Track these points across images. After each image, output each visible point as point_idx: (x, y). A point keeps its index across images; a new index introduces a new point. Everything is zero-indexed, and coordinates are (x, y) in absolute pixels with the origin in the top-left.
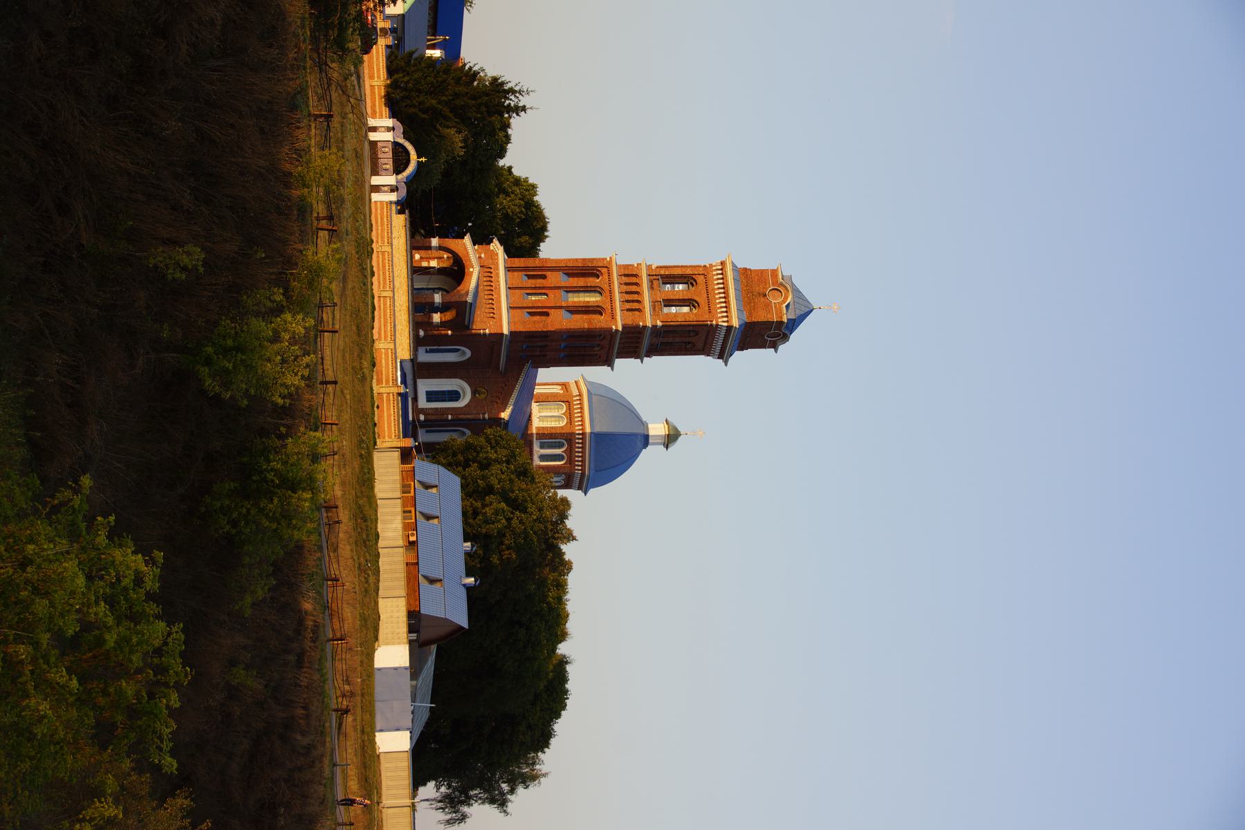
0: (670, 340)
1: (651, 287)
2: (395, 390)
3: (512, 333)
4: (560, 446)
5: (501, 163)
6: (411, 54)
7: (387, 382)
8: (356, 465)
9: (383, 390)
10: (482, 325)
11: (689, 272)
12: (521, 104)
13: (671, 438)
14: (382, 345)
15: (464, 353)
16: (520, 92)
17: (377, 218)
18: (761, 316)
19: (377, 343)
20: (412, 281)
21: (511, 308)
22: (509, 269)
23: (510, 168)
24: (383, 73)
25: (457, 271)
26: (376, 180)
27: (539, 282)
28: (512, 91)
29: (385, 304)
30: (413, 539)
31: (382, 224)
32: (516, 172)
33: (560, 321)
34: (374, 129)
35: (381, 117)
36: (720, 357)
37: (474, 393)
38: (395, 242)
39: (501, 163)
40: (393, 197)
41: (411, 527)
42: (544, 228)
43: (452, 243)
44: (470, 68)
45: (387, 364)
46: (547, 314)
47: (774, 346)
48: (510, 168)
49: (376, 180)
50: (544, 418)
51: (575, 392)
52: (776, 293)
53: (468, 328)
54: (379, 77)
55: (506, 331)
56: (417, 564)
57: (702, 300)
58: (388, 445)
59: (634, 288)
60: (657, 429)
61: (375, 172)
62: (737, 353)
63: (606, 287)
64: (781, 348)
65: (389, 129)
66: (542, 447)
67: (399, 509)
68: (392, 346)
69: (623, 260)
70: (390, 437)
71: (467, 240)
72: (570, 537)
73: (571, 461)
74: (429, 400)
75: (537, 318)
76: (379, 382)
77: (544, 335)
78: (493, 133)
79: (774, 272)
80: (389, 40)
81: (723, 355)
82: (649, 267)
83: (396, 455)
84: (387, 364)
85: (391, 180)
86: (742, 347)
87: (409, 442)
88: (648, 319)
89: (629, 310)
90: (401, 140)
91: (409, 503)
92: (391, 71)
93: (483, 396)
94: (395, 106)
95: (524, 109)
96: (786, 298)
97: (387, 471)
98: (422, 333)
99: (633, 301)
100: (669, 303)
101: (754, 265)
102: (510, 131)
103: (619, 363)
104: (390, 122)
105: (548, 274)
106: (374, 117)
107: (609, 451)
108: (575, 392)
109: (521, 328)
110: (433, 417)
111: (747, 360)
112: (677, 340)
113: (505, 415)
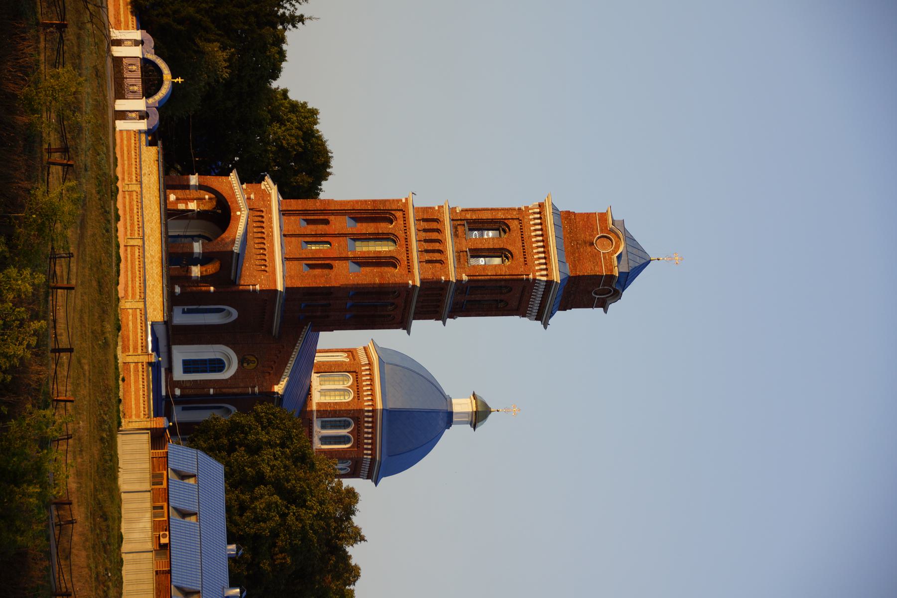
1: (455, 234)
2: (145, 359)
3: (287, 289)
10: (252, 280)
11: (500, 215)
26: (121, 105)
29: (133, 255)
30: (164, 541)
31: (129, 158)
34: (119, 43)
38: (145, 180)
40: (143, 125)
41: (161, 526)
46: (330, 267)
56: (170, 572)
61: (120, 95)
67: (148, 505)
68: (141, 305)
76: (125, 349)
82: (452, 210)
87: (161, 422)
91: (161, 497)
96: (617, 247)
97: (134, 456)
104: (137, 35)
106: (118, 28)
109: (298, 284)
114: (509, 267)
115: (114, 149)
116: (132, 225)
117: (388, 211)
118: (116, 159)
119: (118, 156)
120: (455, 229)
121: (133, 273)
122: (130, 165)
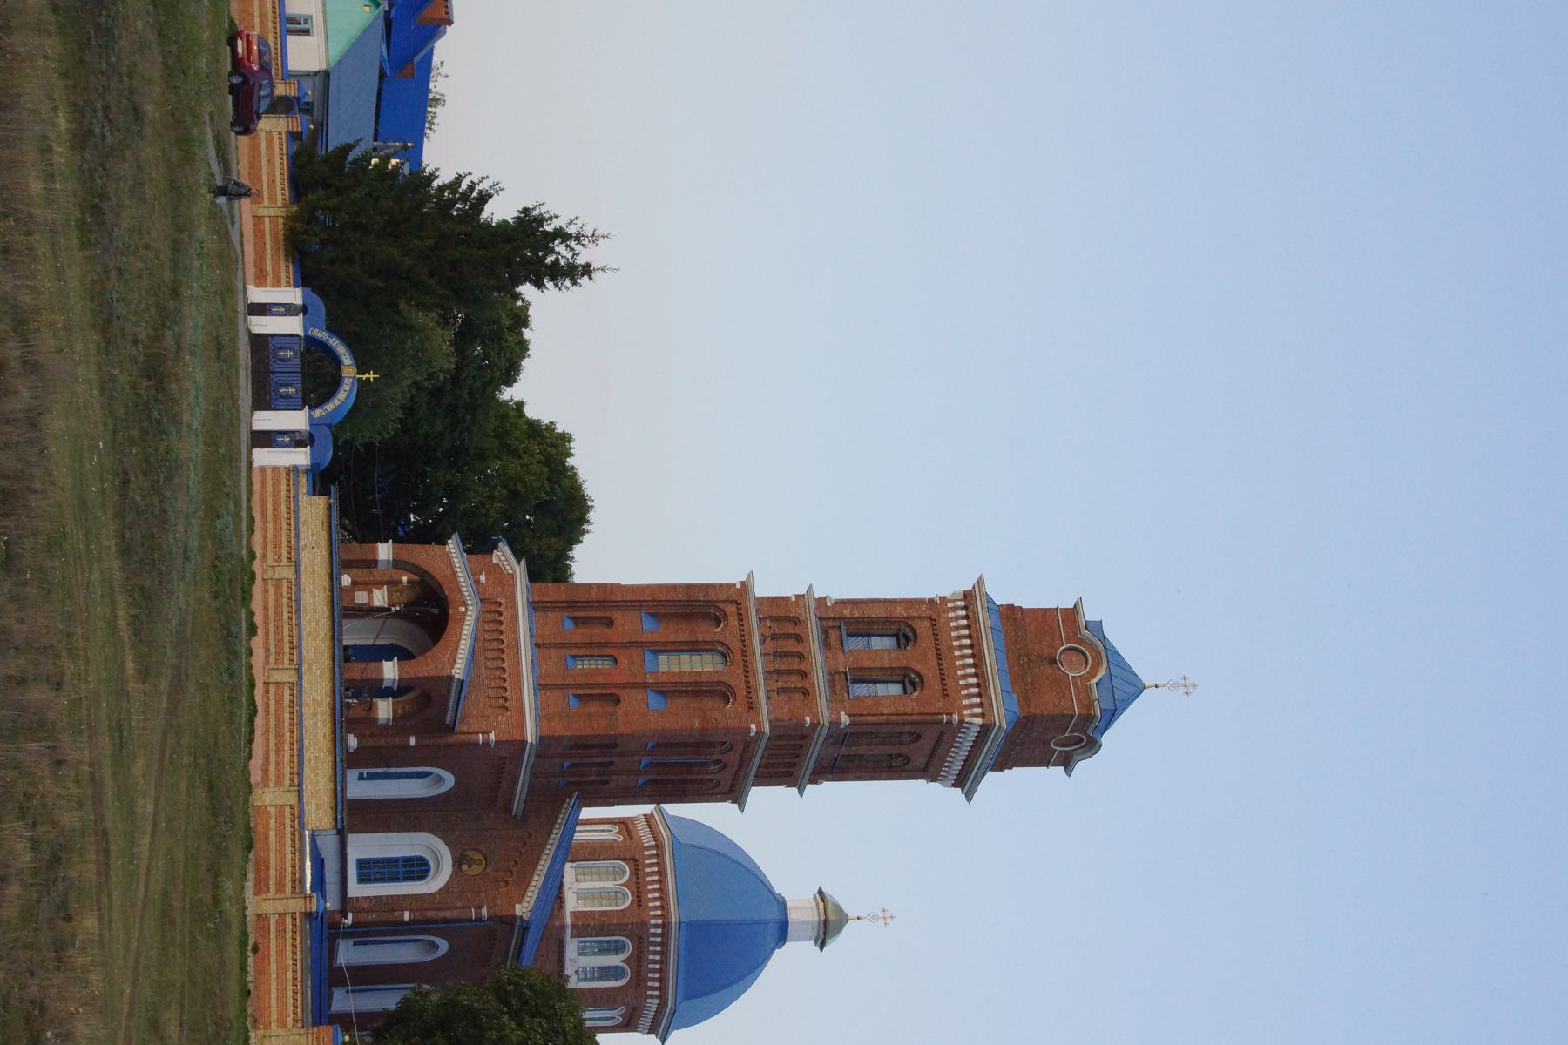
0: (862, 750)
1: (826, 644)
2: (297, 905)
3: (542, 739)
4: (617, 949)
5: (508, 394)
6: (346, 149)
7: (280, 887)
9: (267, 908)
11: (900, 612)
12: (581, 261)
13: (828, 927)
14: (270, 797)
15: (440, 780)
16: (578, 238)
17: (264, 503)
18: (1048, 703)
19: (257, 792)
21: (541, 687)
22: (536, 606)
23: (520, 405)
24: (282, 191)
25: (429, 612)
26: (266, 420)
27: (599, 633)
28: (561, 235)
29: (279, 701)
31: (276, 517)
32: (530, 412)
33: (647, 714)
34: (262, 309)
36: (959, 782)
37: (458, 862)
38: (305, 557)
39: (508, 394)
40: (300, 457)
42: (583, 519)
43: (423, 555)
44: (471, 188)
47: (1067, 763)
48: (520, 405)
49: (266, 420)
50: (587, 889)
51: (648, 840)
52: (1075, 658)
53: (451, 729)
54: (272, 199)
55: (530, 737)
57: (929, 671)
59: (790, 646)
60: (802, 911)
61: (263, 401)
62: (991, 776)
63: (735, 644)
64: (1081, 767)
65: (289, 310)
66: (582, 952)
69: (763, 589)
71: (453, 546)
73: (638, 980)
74: (363, 879)
75: (594, 708)
77: (610, 745)
78: (496, 337)
79: (1072, 614)
80: (296, 123)
81: (965, 781)
82: (821, 601)
86: (1001, 764)
89: (781, 691)
90: (321, 334)
92: (300, 183)
93: (476, 870)
94: (308, 257)
95: (587, 270)
98: (353, 742)
99: (790, 672)
100: (863, 676)
102: (527, 334)
103: (758, 795)
104: (295, 296)
105: (617, 616)
106: (261, 281)
108: (648, 840)
109: (560, 729)
110: (373, 917)
111: (1007, 788)
112: (876, 750)
114: (917, 700)
115: (249, 500)
116: (280, 641)
117: (712, 603)
118: (251, 519)
119: (257, 514)
120: (825, 632)
122: (277, 530)
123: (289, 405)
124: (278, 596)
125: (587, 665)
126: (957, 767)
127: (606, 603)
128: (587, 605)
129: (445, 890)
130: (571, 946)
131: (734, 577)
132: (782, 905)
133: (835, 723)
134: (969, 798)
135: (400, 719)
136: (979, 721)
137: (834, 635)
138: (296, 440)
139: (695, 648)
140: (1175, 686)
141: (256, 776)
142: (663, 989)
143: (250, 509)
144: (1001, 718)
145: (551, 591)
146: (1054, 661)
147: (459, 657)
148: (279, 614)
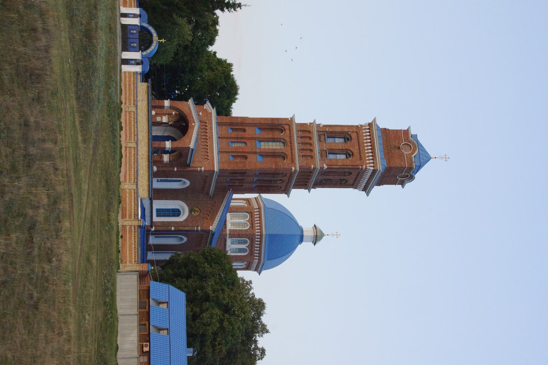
0: (331, 178)
1: (320, 140)
2: (136, 223)
3: (221, 171)
4: (245, 242)
5: (211, 49)
7: (130, 216)
8: (100, 313)
9: (126, 223)
10: (200, 165)
11: (346, 130)
13: (317, 238)
14: (127, 186)
15: (185, 183)
17: (125, 84)
18: (397, 163)
19: (123, 184)
20: (149, 131)
21: (220, 152)
22: (219, 124)
23: (215, 53)
25: (182, 125)
26: (126, 55)
27: (240, 134)
29: (130, 153)
30: (146, 349)
31: (130, 90)
32: (218, 56)
33: (257, 163)
34: (125, 15)
35: (131, 6)
36: (365, 189)
37: (191, 211)
38: (139, 104)
39: (211, 49)
40: (138, 69)
41: (145, 337)
42: (236, 93)
43: (180, 105)
45: (131, 202)
47: (402, 184)
48: (215, 53)
49: (126, 55)
51: (256, 206)
57: (355, 150)
58: (129, 269)
59: (307, 141)
60: (308, 231)
61: (125, 48)
62: (376, 188)
63: (288, 139)
64: (408, 185)
65: (135, 16)
66: (232, 243)
67: (135, 324)
68: (135, 187)
69: (298, 120)
70: (131, 262)
71: (191, 102)
72: (264, 330)
73: (251, 253)
74: (158, 215)
75: (238, 160)
76: (124, 216)
77: (243, 173)
79: (406, 132)
81: (366, 189)
82: (318, 125)
83: (135, 277)
84: (131, 202)
85: (137, 55)
86: (379, 183)
87: (145, 267)
88: (318, 164)
90: (146, 25)
91: (145, 316)
93: (197, 214)
98: (155, 169)
99: (307, 150)
101: (391, 126)
102: (218, 27)
103: (295, 192)
104: (137, 11)
105: (247, 128)
106: (125, 5)
107: (277, 243)
108: (256, 206)
109: (226, 167)
110: (161, 228)
113: (212, 228)
115: (120, 83)
116: (130, 133)
118: (121, 90)
119: (123, 88)
120: (319, 136)
121: (130, 165)
122: (130, 94)
123: (134, 50)
124: (130, 117)
125: (236, 145)
126: (364, 184)
127: (242, 124)
128: (237, 124)
129: (186, 220)
130: (229, 241)
131: (289, 116)
132: (302, 230)
133: (322, 168)
134: (368, 195)
135: (171, 162)
136: (372, 168)
137: (322, 137)
138: (137, 63)
139: (274, 140)
140: (442, 158)
141: (122, 179)
142: (260, 256)
143: (121, 86)
144: (380, 167)
145: (224, 119)
146: (399, 148)
147: (192, 141)
148: (130, 123)
